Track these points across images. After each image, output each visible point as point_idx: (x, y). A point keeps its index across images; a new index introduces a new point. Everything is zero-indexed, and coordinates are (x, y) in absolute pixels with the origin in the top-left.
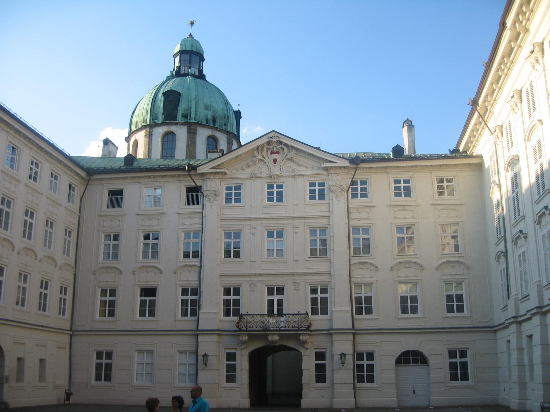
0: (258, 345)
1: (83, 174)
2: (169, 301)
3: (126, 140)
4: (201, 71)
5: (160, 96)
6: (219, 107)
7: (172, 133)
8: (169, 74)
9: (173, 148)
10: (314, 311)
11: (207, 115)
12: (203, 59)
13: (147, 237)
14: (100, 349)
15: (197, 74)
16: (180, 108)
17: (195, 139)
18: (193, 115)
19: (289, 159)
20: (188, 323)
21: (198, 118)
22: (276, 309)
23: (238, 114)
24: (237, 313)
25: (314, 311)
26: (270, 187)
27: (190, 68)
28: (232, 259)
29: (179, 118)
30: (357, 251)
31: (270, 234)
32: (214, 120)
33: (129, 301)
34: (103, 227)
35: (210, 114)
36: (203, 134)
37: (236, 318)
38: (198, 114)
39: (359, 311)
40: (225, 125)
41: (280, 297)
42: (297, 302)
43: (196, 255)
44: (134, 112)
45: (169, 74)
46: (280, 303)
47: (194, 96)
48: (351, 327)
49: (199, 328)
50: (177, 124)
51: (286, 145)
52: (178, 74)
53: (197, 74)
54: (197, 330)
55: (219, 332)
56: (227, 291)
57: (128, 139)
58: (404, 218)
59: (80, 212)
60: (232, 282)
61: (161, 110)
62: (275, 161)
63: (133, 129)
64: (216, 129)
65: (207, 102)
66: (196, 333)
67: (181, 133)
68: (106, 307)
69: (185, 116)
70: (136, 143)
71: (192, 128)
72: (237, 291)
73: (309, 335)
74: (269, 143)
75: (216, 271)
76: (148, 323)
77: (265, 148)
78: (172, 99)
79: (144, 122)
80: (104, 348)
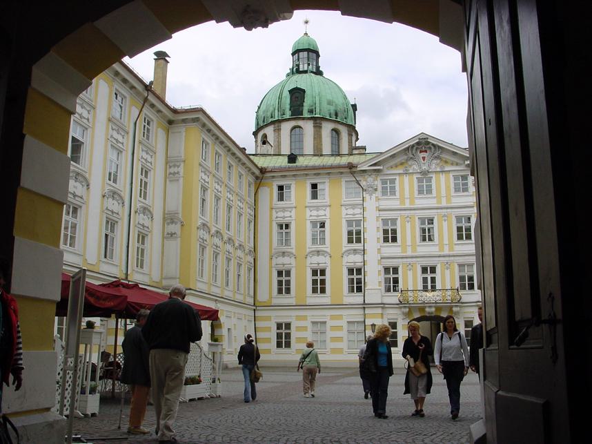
1: (257, 172)
2: (337, 281)
3: (253, 134)
4: (318, 67)
5: (286, 95)
6: (340, 101)
7: (300, 127)
8: (289, 71)
9: (301, 141)
11: (329, 110)
12: (318, 56)
14: (280, 321)
15: (314, 70)
16: (305, 104)
17: (320, 132)
18: (318, 110)
20: (357, 298)
21: (322, 113)
23: (354, 107)
26: (420, 180)
27: (309, 65)
28: (390, 244)
29: (306, 115)
32: (336, 115)
33: (302, 281)
34: (277, 217)
35: (332, 109)
36: (327, 128)
38: (322, 109)
40: (346, 118)
41: (433, 275)
43: (358, 241)
44: (259, 108)
45: (289, 71)
46: (433, 280)
47: (317, 92)
49: (366, 302)
50: (304, 119)
51: (433, 145)
52: (296, 71)
53: (314, 70)
54: (364, 304)
55: (383, 306)
56: (387, 270)
57: (255, 134)
61: (288, 107)
62: (424, 158)
63: (261, 124)
65: (329, 97)
66: (364, 306)
67: (308, 127)
68: (282, 285)
69: (311, 111)
71: (318, 121)
73: (460, 307)
74: (418, 143)
75: (374, 255)
76: (319, 299)
77: (415, 148)
78: (297, 95)
79: (272, 117)
80: (283, 320)
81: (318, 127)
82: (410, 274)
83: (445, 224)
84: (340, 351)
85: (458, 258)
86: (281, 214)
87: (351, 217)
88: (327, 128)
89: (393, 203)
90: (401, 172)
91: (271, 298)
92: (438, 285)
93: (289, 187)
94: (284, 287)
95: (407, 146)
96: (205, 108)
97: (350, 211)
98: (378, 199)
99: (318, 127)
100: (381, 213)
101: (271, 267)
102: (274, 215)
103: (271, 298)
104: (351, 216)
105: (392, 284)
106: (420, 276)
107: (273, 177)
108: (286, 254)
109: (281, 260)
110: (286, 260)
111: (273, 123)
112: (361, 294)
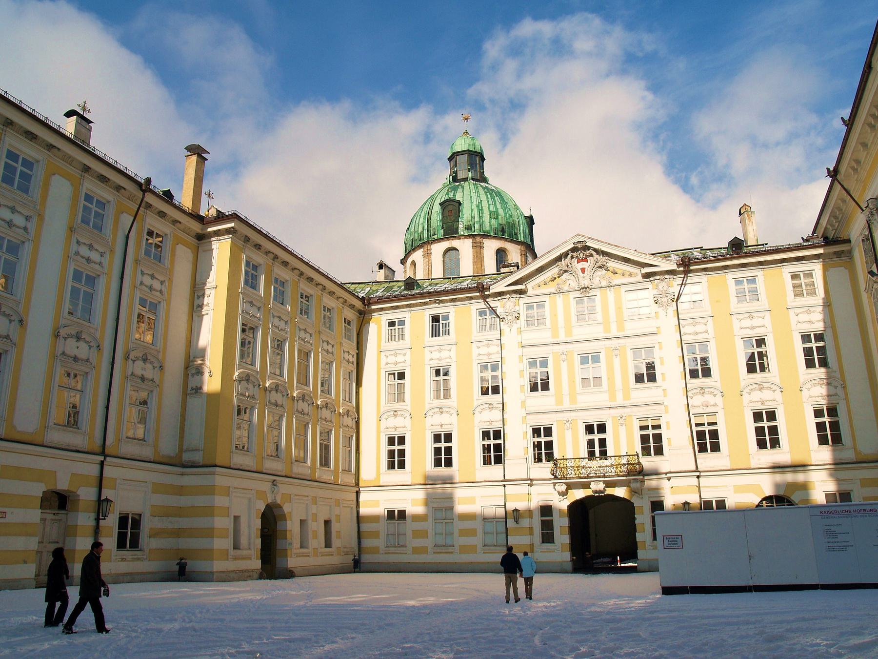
0: (579, 494)
1: (358, 304)
5: (437, 208)
7: (456, 249)
10: (646, 451)
12: (483, 159)
13: (438, 373)
18: (477, 226)
19: (600, 267)
20: (495, 471)
22: (598, 449)
23: (530, 220)
24: (550, 457)
25: (646, 451)
28: (540, 393)
29: (462, 230)
30: (694, 374)
31: (584, 360)
34: (387, 364)
37: (551, 464)
39: (703, 449)
41: (602, 436)
42: (623, 443)
43: (496, 390)
46: (603, 442)
48: (694, 468)
50: (459, 237)
56: (536, 432)
58: (753, 328)
59: (358, 349)
60: (541, 422)
62: (583, 270)
64: (506, 240)
67: (465, 247)
69: (468, 228)
70: (414, 264)
72: (548, 431)
81: (478, 248)
82: (568, 434)
83: (617, 362)
84: (472, 549)
85: (635, 409)
86: (392, 359)
87: (484, 359)
88: (491, 246)
89: (541, 335)
90: (552, 290)
91: (378, 474)
92: (610, 451)
93: (402, 323)
94: (397, 460)
95: (558, 254)
96: (243, 214)
97: (484, 350)
98: (520, 331)
99: (478, 248)
100: (525, 349)
101: (379, 432)
102: (384, 360)
103: (378, 474)
104: (486, 357)
105: (544, 451)
106: (584, 438)
107: (382, 309)
108: (399, 413)
109: (392, 422)
110: (399, 422)
111: (420, 246)
112: (500, 466)
